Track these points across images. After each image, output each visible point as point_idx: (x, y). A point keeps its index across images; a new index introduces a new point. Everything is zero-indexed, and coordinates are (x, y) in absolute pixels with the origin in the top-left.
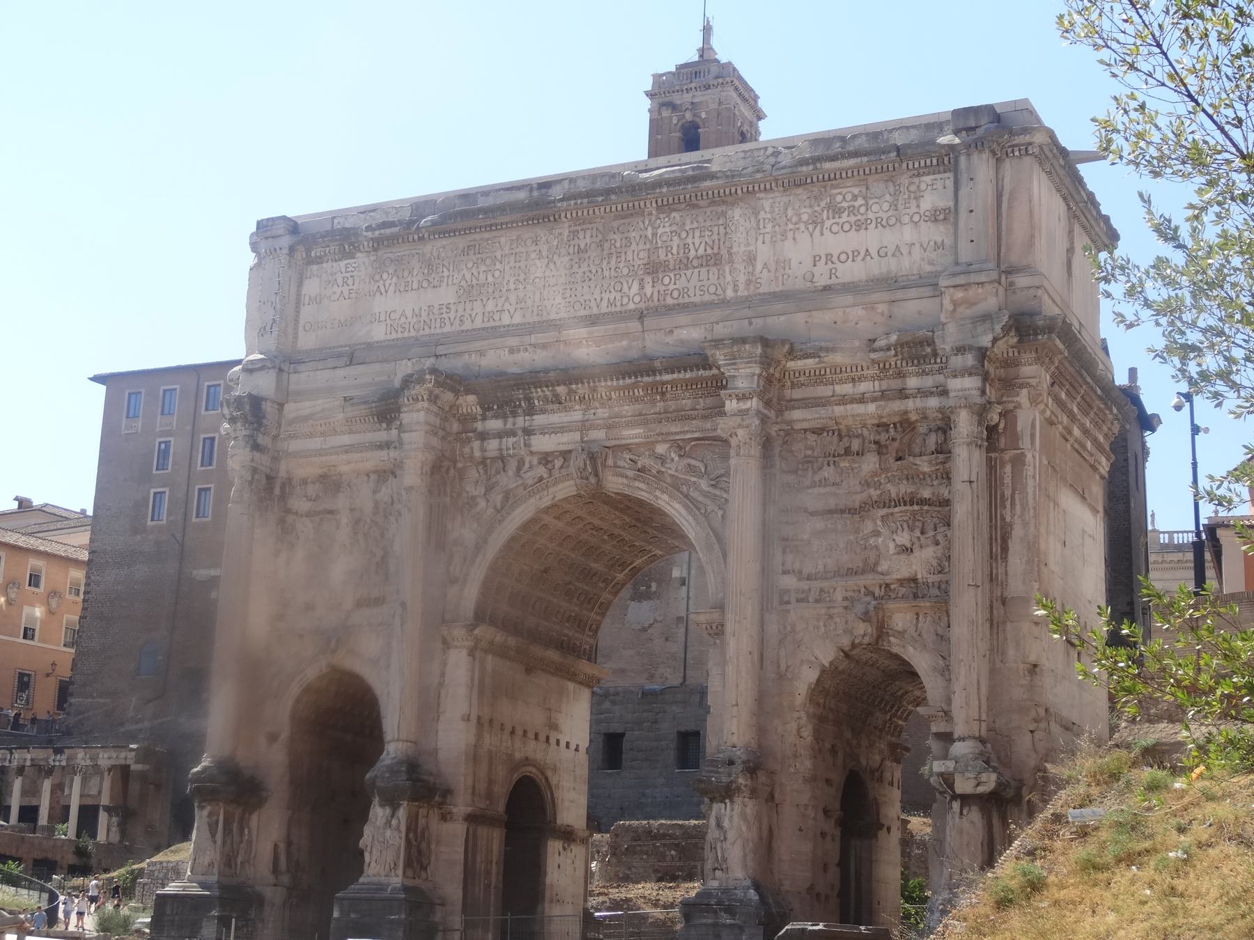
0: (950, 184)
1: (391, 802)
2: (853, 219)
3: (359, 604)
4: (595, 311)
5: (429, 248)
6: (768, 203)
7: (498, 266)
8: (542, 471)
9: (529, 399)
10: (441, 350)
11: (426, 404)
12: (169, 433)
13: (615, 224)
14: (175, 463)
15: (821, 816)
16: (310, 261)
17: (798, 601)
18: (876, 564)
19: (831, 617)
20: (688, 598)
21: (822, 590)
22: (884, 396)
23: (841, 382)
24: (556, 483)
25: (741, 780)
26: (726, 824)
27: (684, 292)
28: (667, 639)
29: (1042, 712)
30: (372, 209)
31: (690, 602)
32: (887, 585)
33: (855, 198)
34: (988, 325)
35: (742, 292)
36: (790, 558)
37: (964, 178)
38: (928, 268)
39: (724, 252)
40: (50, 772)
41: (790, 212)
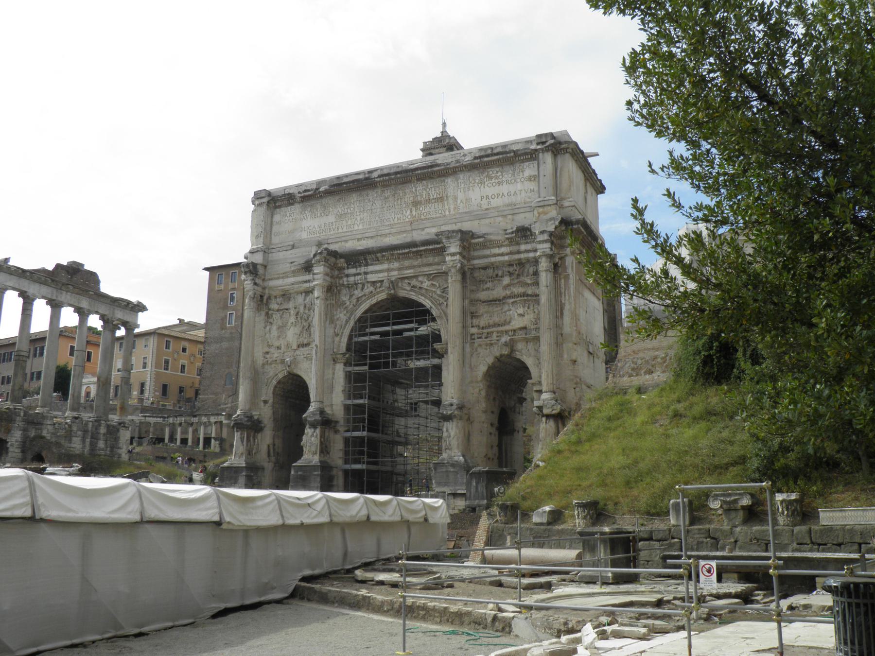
0: (536, 165)
1: (314, 426)
2: (497, 181)
3: (299, 346)
4: (392, 222)
5: (324, 201)
7: (352, 206)
8: (372, 289)
9: (365, 259)
10: (330, 241)
11: (323, 263)
12: (233, 289)
14: (237, 301)
15: (489, 426)
16: (276, 207)
17: (478, 338)
18: (510, 322)
19: (491, 344)
21: (488, 333)
22: (511, 253)
23: (494, 247)
24: (378, 293)
25: (456, 412)
26: (450, 431)
27: (429, 213)
29: (578, 380)
30: (301, 185)
32: (515, 331)
33: (497, 172)
34: (553, 222)
36: (474, 321)
37: (541, 162)
38: (528, 200)
39: (444, 195)
40: (192, 424)
41: (471, 179)
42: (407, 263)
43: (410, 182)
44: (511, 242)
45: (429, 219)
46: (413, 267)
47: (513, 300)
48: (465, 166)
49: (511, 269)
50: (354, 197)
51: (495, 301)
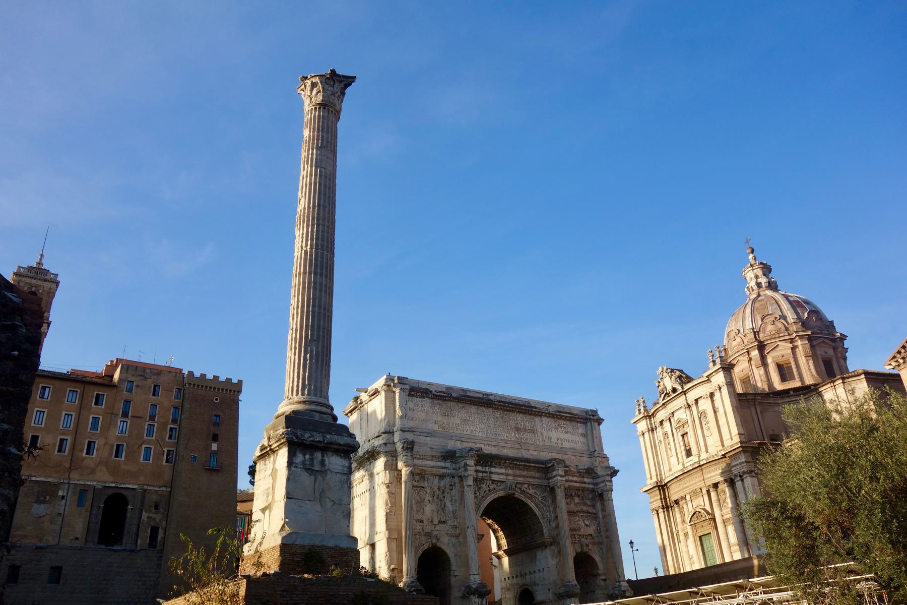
4: (503, 438)
6: (544, 419)
8: (494, 486)
10: (463, 439)
13: (506, 412)
19: (575, 543)
20: (65, 505)
23: (570, 476)
27: (526, 439)
28: (51, 523)
31: (66, 507)
33: (564, 424)
35: (541, 443)
37: (593, 429)
38: (583, 449)
42: (518, 472)
43: (513, 411)
44: (581, 474)
45: (528, 443)
46: (523, 476)
47: (581, 514)
48: (549, 413)
49: (579, 493)
50: (473, 409)
51: (572, 512)
